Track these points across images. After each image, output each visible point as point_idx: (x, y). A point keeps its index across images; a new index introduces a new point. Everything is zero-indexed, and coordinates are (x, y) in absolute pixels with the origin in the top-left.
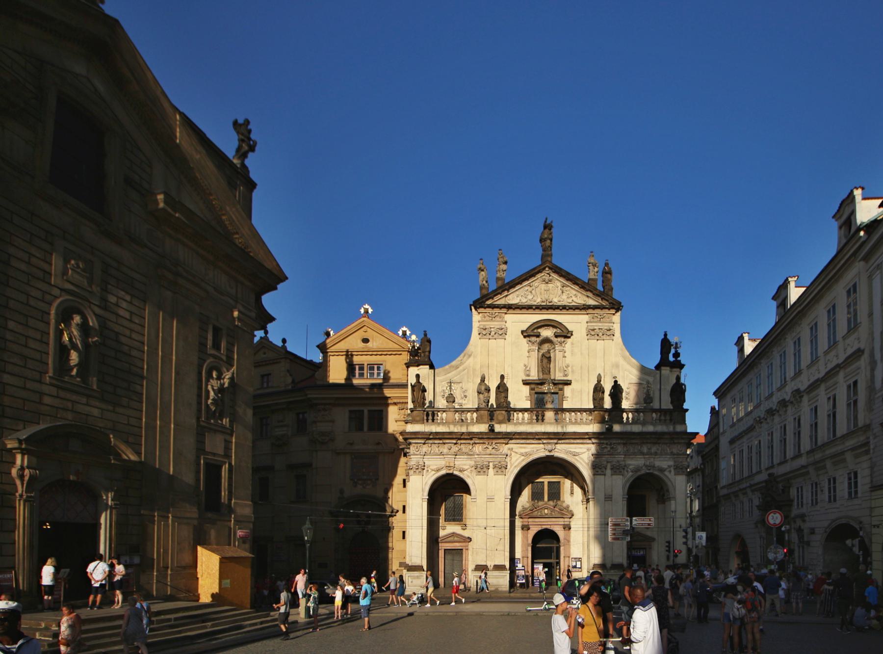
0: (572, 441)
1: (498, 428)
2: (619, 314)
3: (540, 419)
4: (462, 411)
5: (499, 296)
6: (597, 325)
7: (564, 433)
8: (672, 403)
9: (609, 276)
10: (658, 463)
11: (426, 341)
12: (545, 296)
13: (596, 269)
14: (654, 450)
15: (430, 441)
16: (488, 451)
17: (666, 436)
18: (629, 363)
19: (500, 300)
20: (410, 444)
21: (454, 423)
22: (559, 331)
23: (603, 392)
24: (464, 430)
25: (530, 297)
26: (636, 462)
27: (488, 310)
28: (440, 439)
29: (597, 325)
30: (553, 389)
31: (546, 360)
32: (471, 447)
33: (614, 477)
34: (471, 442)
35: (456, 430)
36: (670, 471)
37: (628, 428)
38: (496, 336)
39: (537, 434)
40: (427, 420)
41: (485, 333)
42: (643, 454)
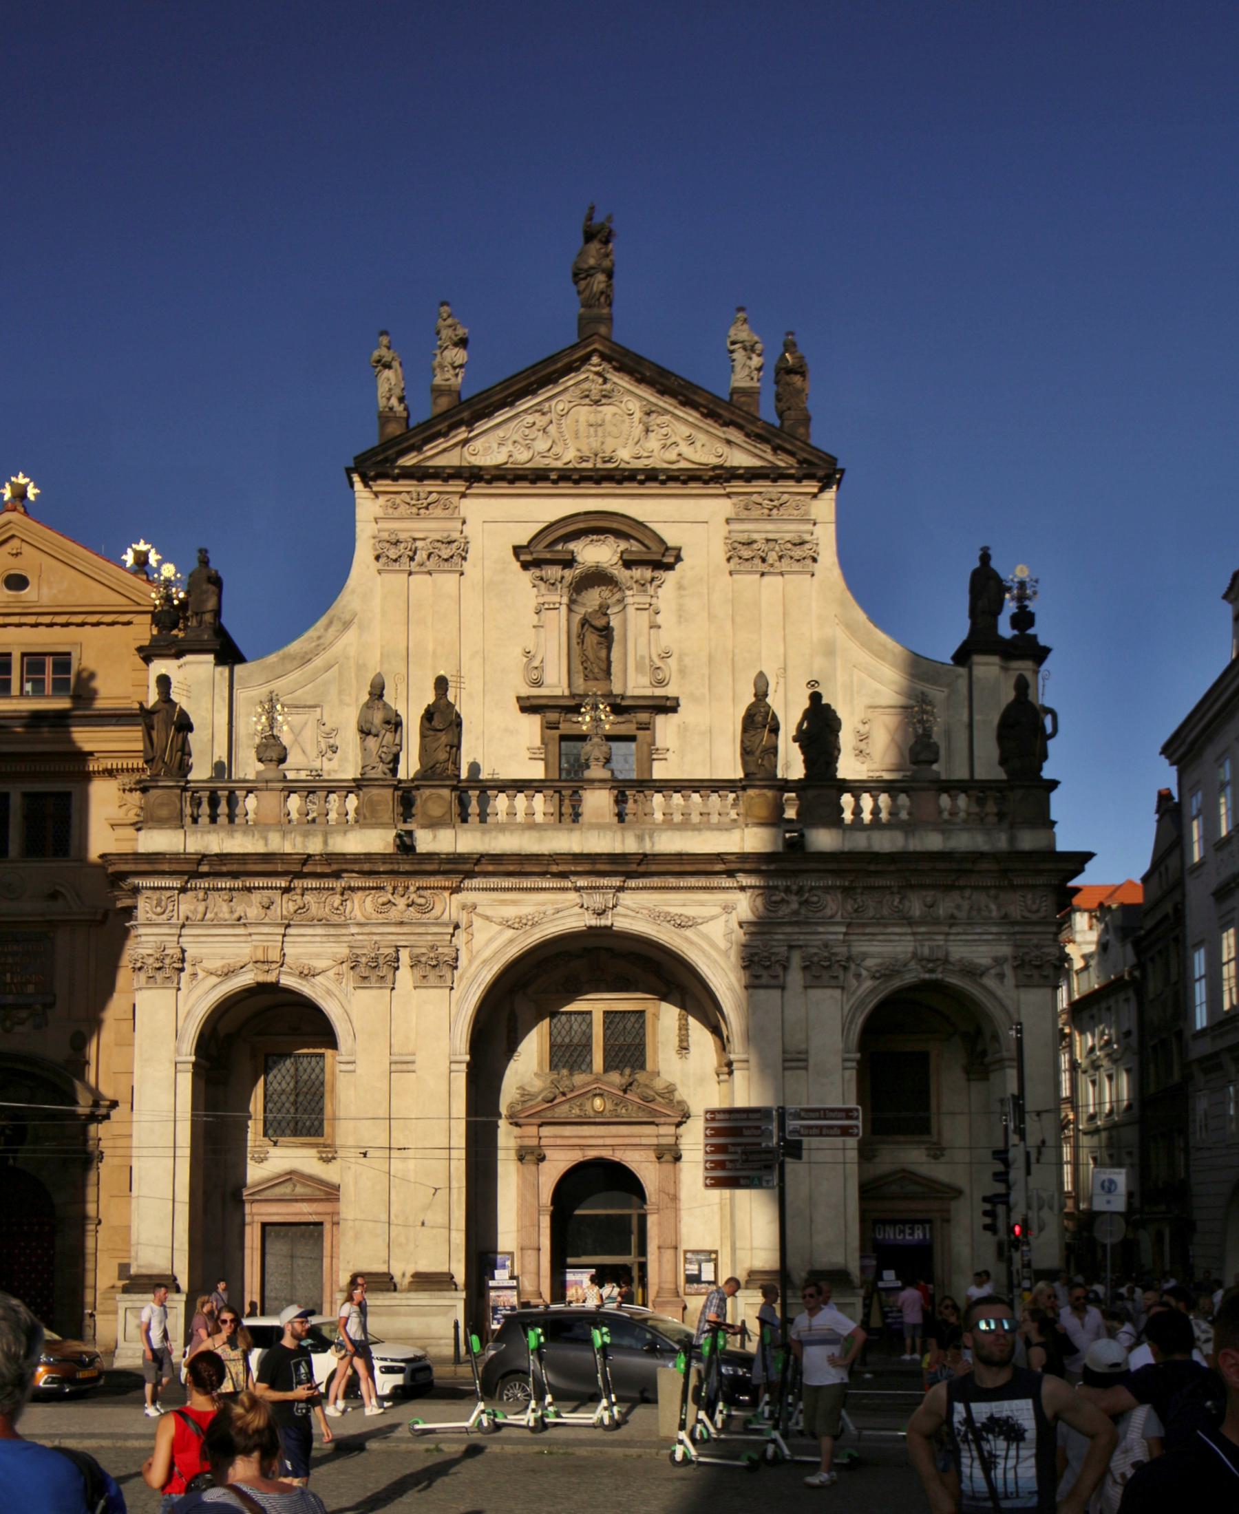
0: (672, 882)
1: (426, 841)
2: (831, 494)
3: (570, 814)
4: (316, 787)
5: (441, 443)
6: (759, 530)
7: (644, 858)
8: (1003, 762)
9: (797, 379)
10: (959, 951)
11: (207, 579)
12: (589, 444)
13: (756, 361)
14: (945, 906)
15: (203, 883)
16: (394, 914)
17: (984, 866)
18: (866, 645)
19: (442, 454)
20: (136, 891)
21: (284, 824)
22: (635, 546)
23: (775, 730)
24: (314, 846)
25: (542, 445)
26: (887, 949)
27: (404, 485)
28: (235, 875)
29: (759, 530)
30: (610, 722)
31: (595, 639)
32: (337, 900)
33: (816, 994)
34: (339, 884)
35: (288, 849)
36: (1001, 977)
37: (860, 842)
38: (430, 565)
39: (554, 858)
40: (195, 820)
41: (398, 555)
42: (910, 922)
